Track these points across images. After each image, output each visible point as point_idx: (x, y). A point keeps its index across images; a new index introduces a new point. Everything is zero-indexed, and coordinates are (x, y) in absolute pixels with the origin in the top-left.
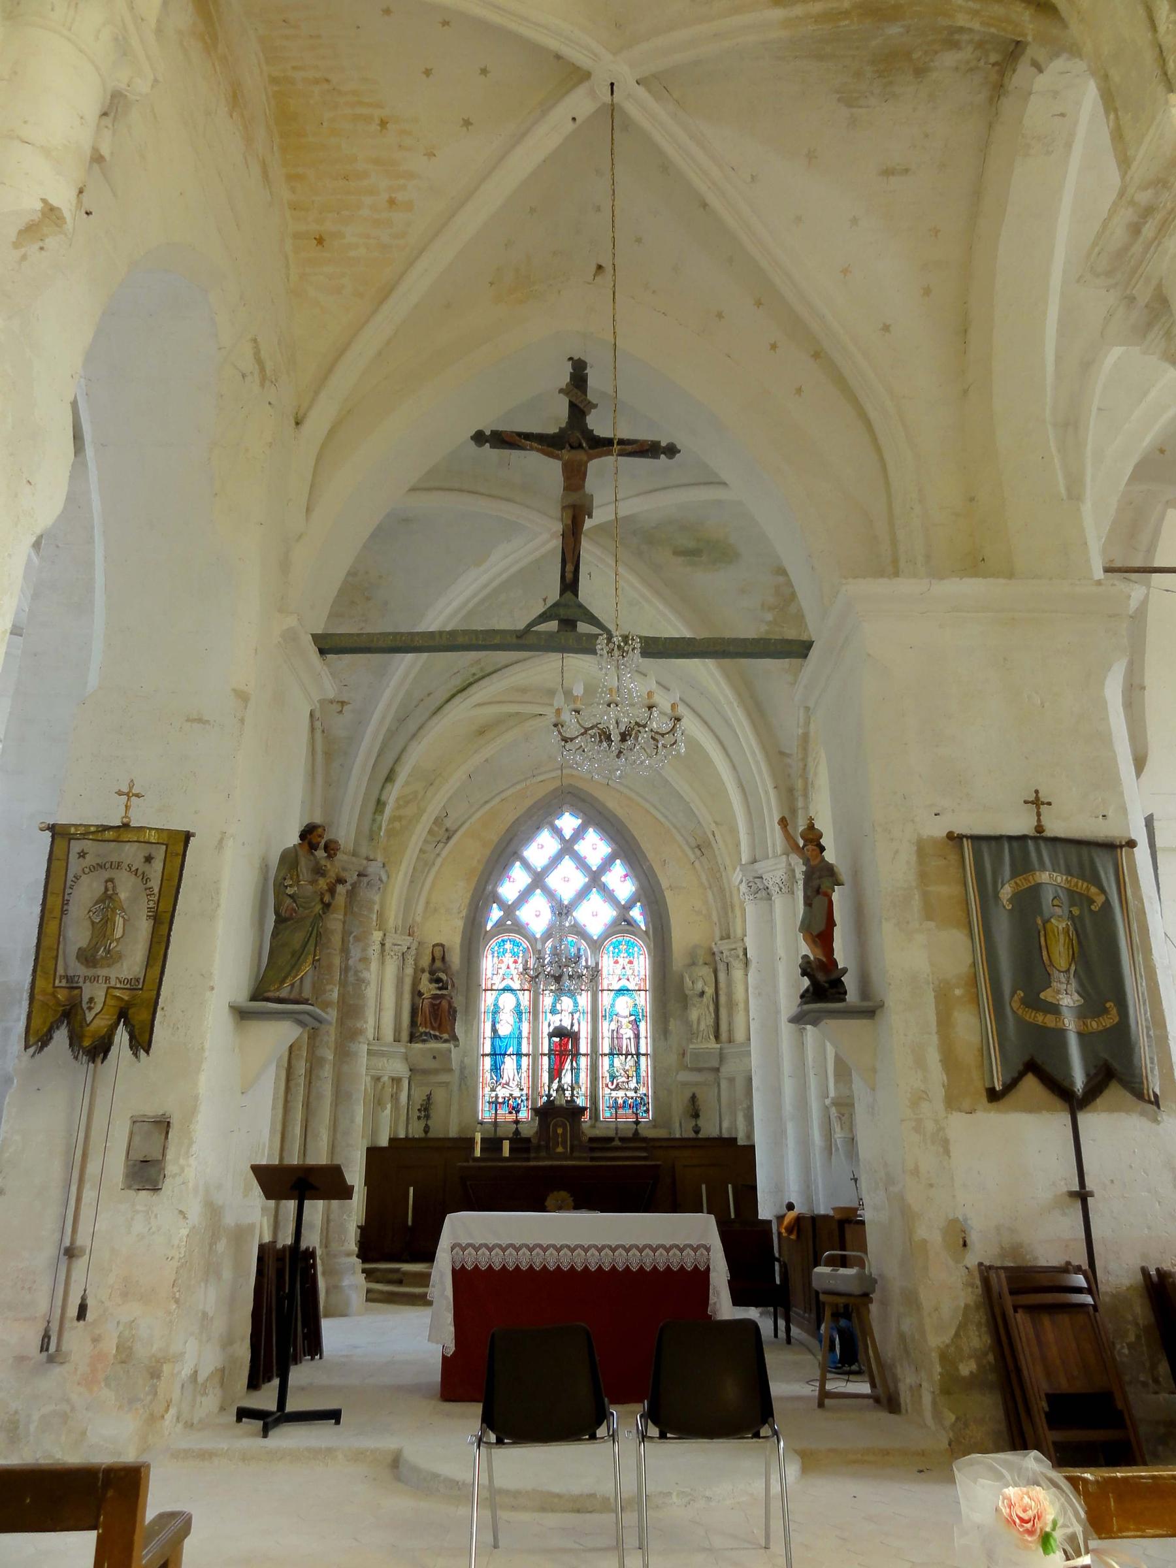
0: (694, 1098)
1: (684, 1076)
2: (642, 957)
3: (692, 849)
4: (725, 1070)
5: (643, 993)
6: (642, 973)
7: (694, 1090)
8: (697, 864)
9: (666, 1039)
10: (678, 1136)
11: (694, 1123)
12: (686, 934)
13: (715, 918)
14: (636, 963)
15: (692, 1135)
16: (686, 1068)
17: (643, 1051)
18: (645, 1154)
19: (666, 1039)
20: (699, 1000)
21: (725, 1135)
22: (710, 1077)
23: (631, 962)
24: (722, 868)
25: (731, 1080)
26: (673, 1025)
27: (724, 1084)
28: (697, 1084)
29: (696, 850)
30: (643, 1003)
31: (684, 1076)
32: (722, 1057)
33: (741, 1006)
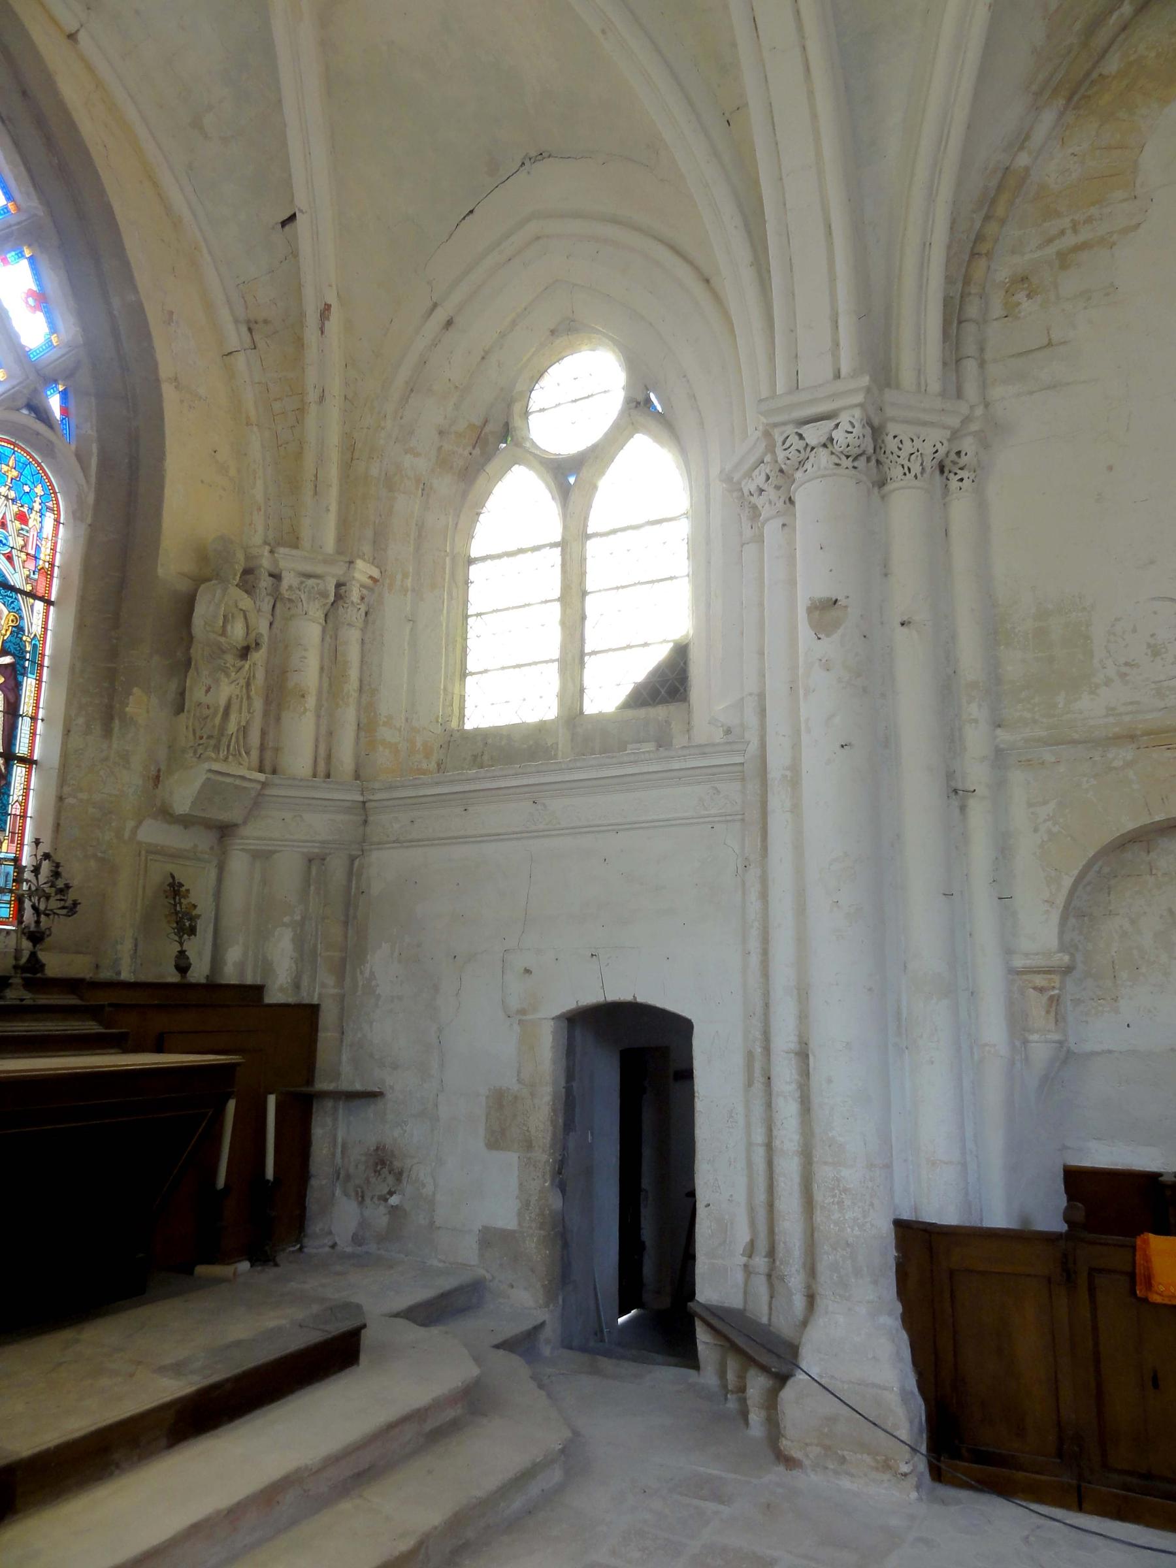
0: (175, 889)
1: (153, 833)
2: (49, 519)
3: (236, 321)
4: (253, 834)
5: (39, 606)
6: (45, 553)
7: (170, 868)
8: (240, 362)
9: (108, 732)
10: (126, 975)
11: (177, 948)
12: (195, 505)
13: (258, 492)
14: (33, 518)
15: (173, 977)
16: (166, 814)
17: (22, 748)
18: (91, 1027)
19: (108, 732)
20: (239, 663)
21: (230, 975)
22: (203, 841)
23: (22, 518)
24: (312, 396)
25: (262, 856)
26: (143, 707)
27: (238, 863)
28: (175, 856)
29: (244, 329)
30: (37, 629)
31: (153, 833)
32: (257, 804)
33: (311, 702)
